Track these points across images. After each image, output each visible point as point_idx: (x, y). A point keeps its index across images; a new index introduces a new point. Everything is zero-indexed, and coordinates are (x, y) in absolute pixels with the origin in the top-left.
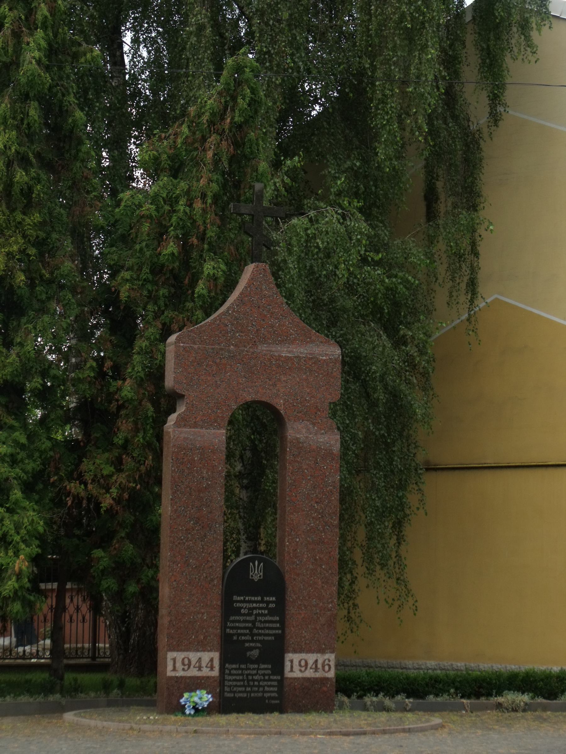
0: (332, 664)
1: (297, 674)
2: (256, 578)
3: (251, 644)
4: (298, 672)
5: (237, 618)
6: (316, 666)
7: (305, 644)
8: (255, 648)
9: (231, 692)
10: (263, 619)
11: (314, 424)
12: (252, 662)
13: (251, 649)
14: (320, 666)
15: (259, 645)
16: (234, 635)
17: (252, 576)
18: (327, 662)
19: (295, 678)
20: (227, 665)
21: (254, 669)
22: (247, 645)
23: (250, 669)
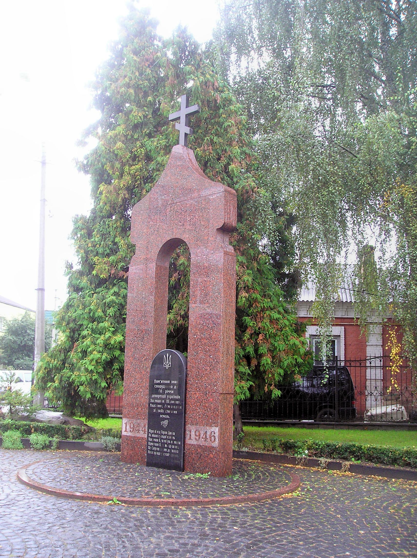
0: (217, 435)
1: (193, 442)
2: (167, 367)
3: (164, 416)
4: (194, 440)
5: (156, 396)
6: (206, 437)
7: (199, 418)
8: (166, 419)
9: (151, 450)
10: (171, 397)
11: (206, 247)
12: (165, 430)
13: (164, 419)
14: (208, 436)
15: (168, 417)
16: (154, 408)
17: (165, 365)
18: (213, 434)
19: (192, 445)
20: (150, 430)
21: (165, 435)
22: (161, 416)
23: (162, 434)
